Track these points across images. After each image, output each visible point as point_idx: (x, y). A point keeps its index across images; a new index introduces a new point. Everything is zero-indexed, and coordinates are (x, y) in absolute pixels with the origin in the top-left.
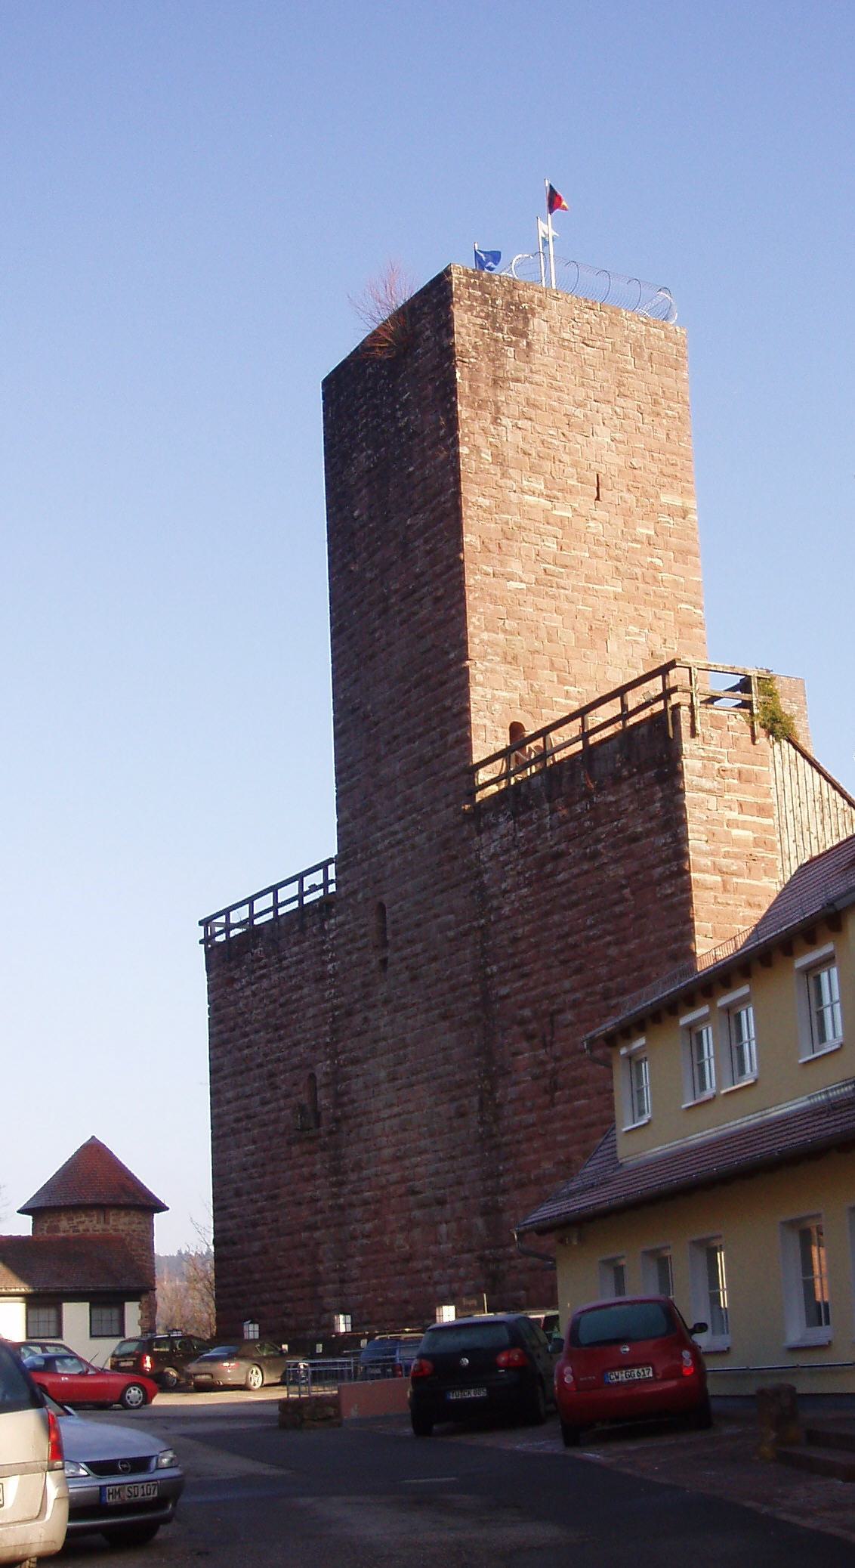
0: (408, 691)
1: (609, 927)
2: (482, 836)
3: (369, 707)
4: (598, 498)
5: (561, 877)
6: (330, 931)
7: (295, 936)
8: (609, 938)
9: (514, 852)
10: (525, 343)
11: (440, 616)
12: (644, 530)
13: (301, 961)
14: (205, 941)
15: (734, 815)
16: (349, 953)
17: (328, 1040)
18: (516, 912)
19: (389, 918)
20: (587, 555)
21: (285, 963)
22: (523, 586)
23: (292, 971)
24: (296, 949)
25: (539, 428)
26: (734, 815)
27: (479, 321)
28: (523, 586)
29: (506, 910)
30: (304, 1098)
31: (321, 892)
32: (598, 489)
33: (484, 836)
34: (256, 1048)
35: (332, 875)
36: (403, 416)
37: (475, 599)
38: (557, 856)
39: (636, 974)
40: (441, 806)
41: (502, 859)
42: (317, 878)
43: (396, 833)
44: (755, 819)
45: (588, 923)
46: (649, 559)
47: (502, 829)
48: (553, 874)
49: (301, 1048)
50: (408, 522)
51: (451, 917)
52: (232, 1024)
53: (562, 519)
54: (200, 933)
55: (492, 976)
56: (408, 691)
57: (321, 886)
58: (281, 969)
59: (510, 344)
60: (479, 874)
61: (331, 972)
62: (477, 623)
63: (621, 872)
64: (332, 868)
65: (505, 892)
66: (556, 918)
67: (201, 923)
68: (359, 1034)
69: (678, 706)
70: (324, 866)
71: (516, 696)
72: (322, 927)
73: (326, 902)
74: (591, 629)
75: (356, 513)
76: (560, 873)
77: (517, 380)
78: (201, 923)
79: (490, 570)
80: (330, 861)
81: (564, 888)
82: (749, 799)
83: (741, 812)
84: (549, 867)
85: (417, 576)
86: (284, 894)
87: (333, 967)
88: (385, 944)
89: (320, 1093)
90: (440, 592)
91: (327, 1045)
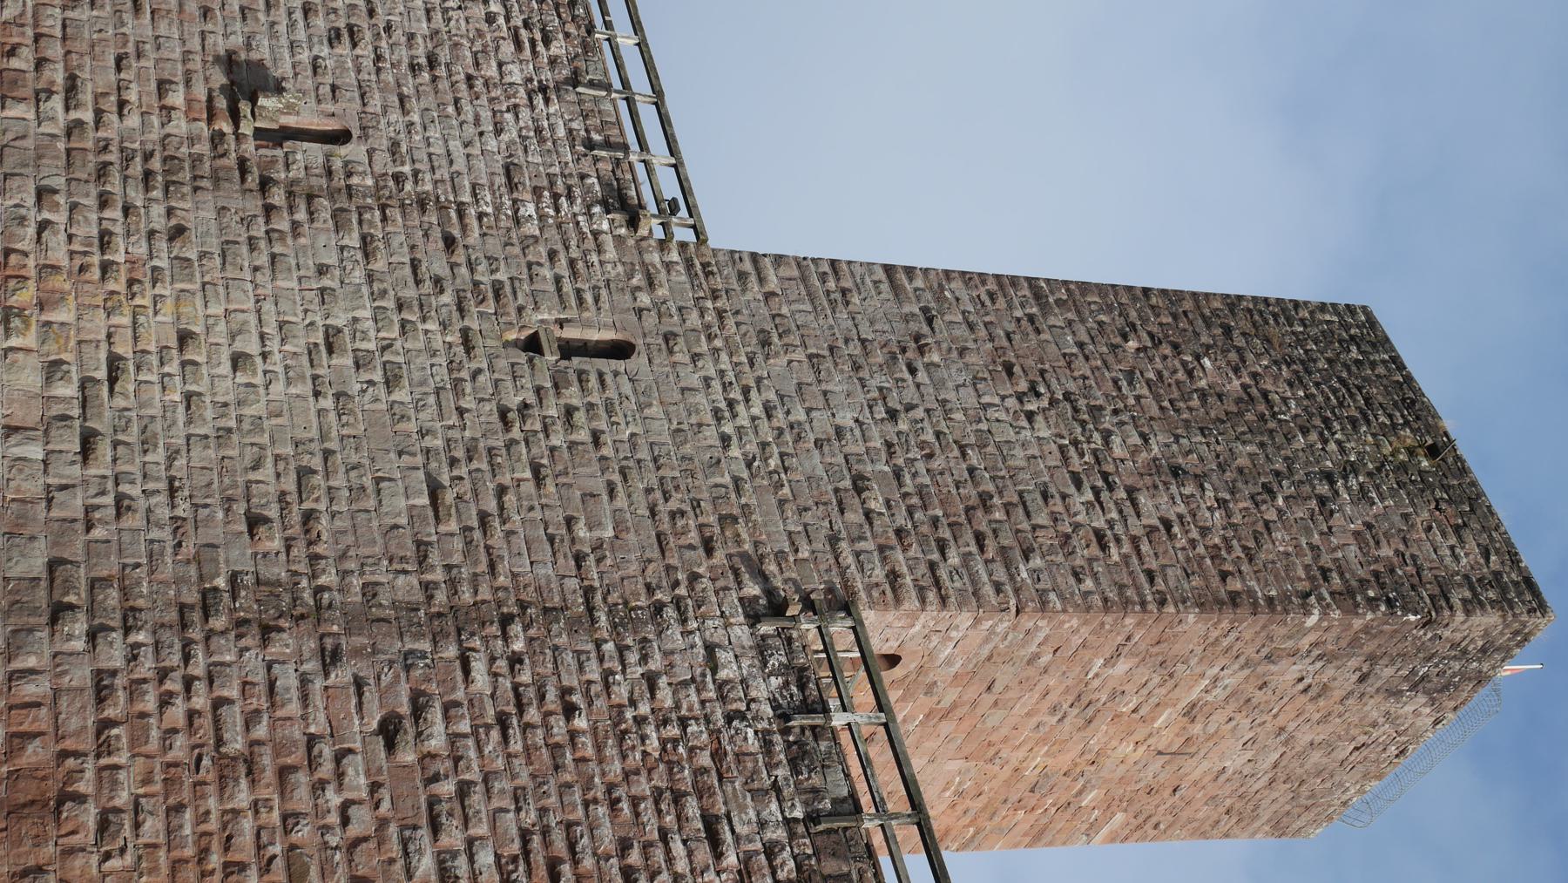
3: (936, 358)
6: (590, 216)
7: (583, 133)
13: (542, 141)
19: (602, 364)
22: (1090, 676)
36: (1348, 489)
37: (1102, 624)
55: (505, 637)
68: (415, 265)
85: (1131, 491)
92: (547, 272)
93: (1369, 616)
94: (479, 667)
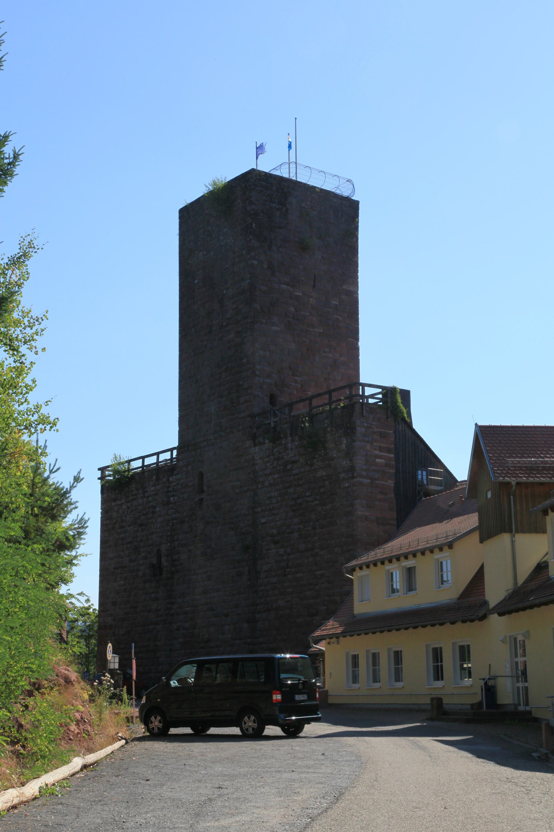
1: (318, 497)
2: (256, 447)
4: (314, 287)
8: (317, 502)
9: (272, 457)
10: (285, 209)
12: (335, 302)
14: (101, 479)
15: (377, 452)
17: (169, 534)
20: (308, 314)
21: (146, 494)
23: (150, 499)
24: (153, 488)
26: (377, 452)
30: (154, 561)
32: (314, 282)
34: (128, 534)
38: (294, 462)
39: (329, 520)
41: (266, 459)
42: (167, 456)
44: (386, 454)
45: (307, 494)
46: (336, 316)
50: (224, 292)
52: (115, 521)
54: (99, 474)
61: (173, 502)
62: (258, 347)
63: (324, 473)
65: (267, 475)
66: (292, 490)
67: (99, 469)
70: (171, 450)
72: (168, 480)
74: (308, 350)
75: (196, 281)
76: (294, 470)
78: (99, 469)
80: (174, 448)
81: (296, 477)
82: (383, 445)
83: (380, 451)
84: (289, 467)
87: (174, 499)
88: (203, 491)
89: (164, 559)
90: (240, 329)
93: (253, 242)
94: (263, 520)
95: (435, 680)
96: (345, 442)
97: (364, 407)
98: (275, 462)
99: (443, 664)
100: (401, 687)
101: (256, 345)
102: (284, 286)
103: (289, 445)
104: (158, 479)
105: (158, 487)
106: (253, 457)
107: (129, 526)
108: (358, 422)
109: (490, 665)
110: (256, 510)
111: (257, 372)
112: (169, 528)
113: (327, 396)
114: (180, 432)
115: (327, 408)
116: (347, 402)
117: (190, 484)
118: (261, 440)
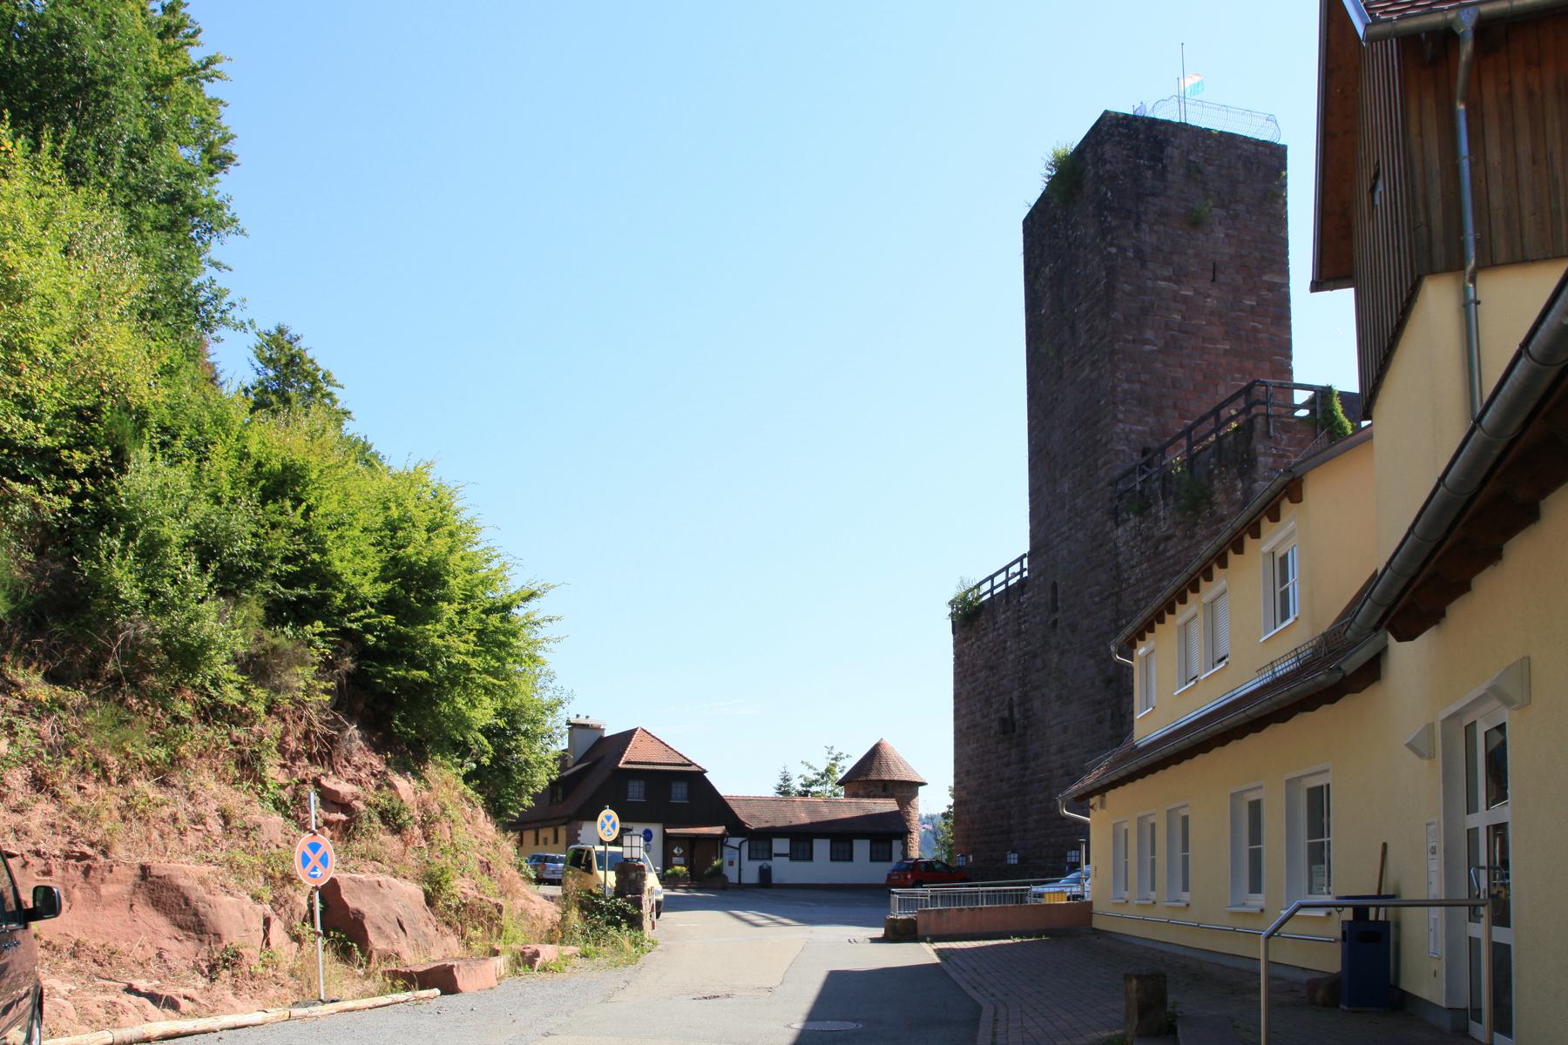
0: (1074, 431)
5: (1168, 554)
6: (1024, 603)
9: (1139, 538)
11: (1094, 375)
16: (1035, 617)
18: (1137, 581)
21: (997, 626)
22: (1155, 348)
23: (1001, 631)
24: (1003, 616)
25: (1170, 231)
27: (1125, 152)
28: (1155, 348)
29: (1132, 581)
31: (1018, 577)
33: (1120, 530)
35: (1026, 565)
38: (1168, 538)
40: (1092, 511)
41: (1131, 544)
42: (1016, 568)
43: (1063, 533)
47: (1132, 524)
48: (1165, 551)
49: (1005, 681)
51: (1098, 588)
53: (1186, 297)
56: (1074, 431)
57: (1019, 573)
58: (994, 630)
59: (1149, 168)
60: (1117, 555)
64: (1025, 561)
65: (1133, 567)
69: (1255, 416)
70: (1020, 560)
71: (1147, 429)
73: (1022, 582)
77: (1153, 195)
79: (1131, 338)
80: (1024, 556)
81: (1171, 561)
84: (1161, 548)
86: (997, 580)
88: (1055, 609)
91: (1020, 678)
92: (1038, 619)
95: (1251, 892)
96: (1240, 485)
97: (1271, 420)
98: (1143, 545)
99: (1263, 846)
100: (1184, 905)
101: (1118, 374)
102: (1162, 283)
103: (1161, 514)
104: (1008, 602)
105: (1009, 613)
106: (1115, 544)
107: (981, 671)
108: (1260, 448)
109: (1385, 845)
110: (1120, 623)
111: (1121, 416)
112: (1020, 667)
113: (1212, 419)
114: (1031, 531)
115: (1212, 438)
116: (1242, 418)
117: (1043, 601)
118: (1125, 516)
